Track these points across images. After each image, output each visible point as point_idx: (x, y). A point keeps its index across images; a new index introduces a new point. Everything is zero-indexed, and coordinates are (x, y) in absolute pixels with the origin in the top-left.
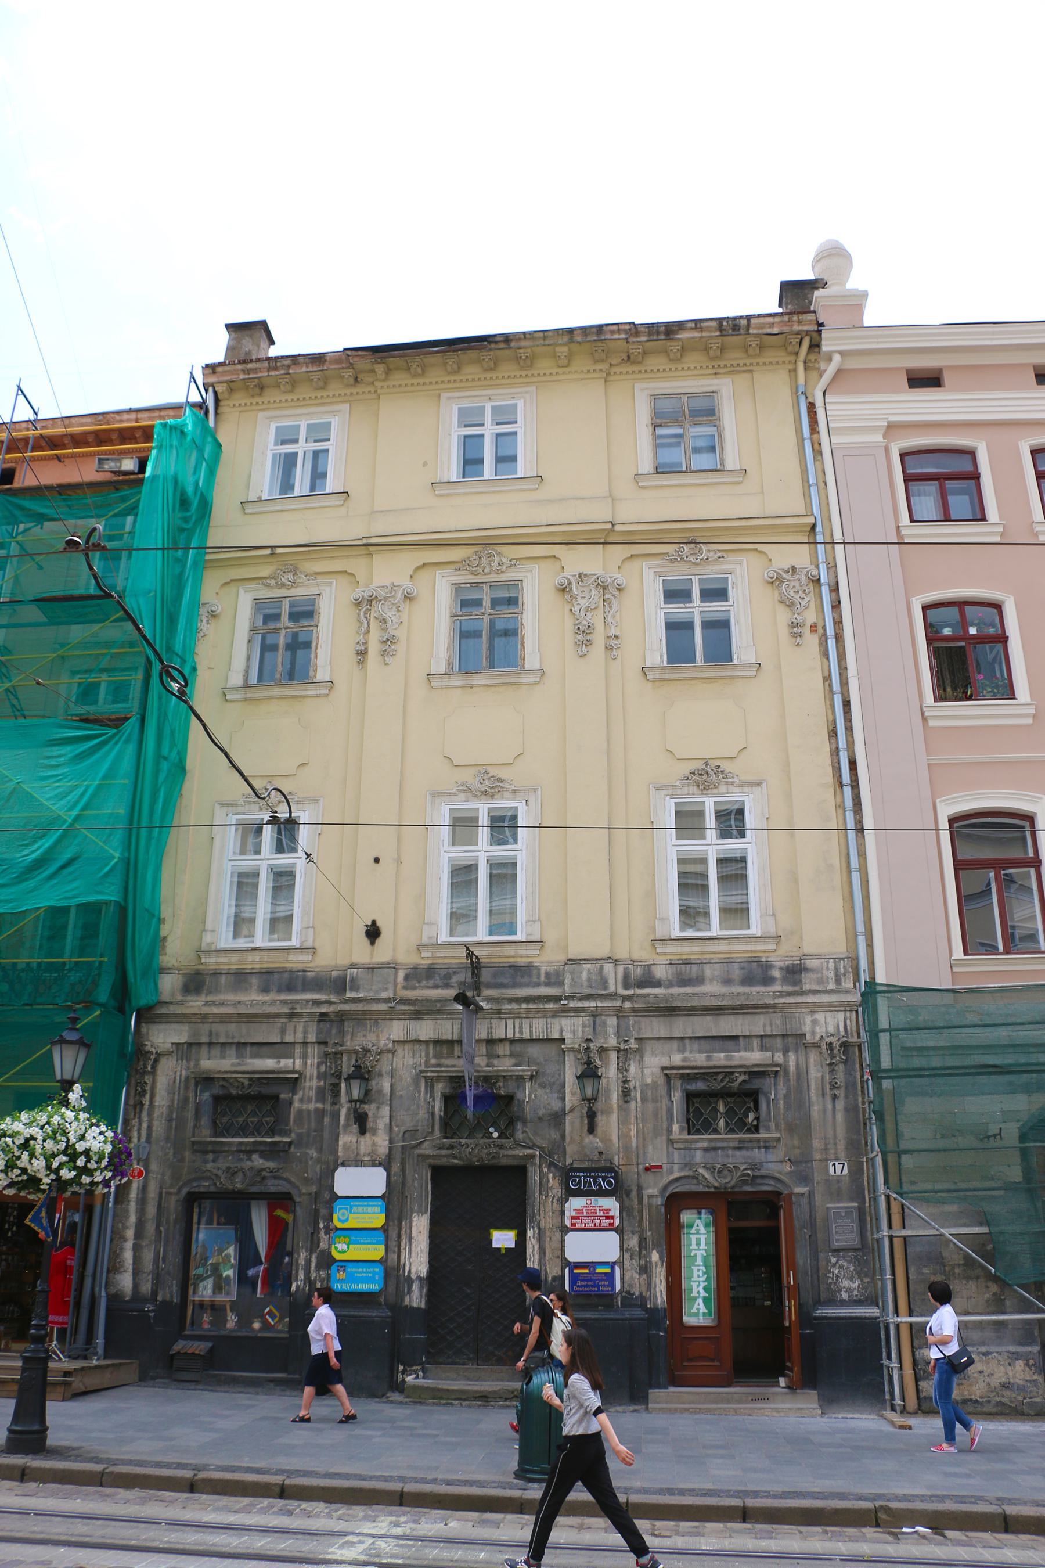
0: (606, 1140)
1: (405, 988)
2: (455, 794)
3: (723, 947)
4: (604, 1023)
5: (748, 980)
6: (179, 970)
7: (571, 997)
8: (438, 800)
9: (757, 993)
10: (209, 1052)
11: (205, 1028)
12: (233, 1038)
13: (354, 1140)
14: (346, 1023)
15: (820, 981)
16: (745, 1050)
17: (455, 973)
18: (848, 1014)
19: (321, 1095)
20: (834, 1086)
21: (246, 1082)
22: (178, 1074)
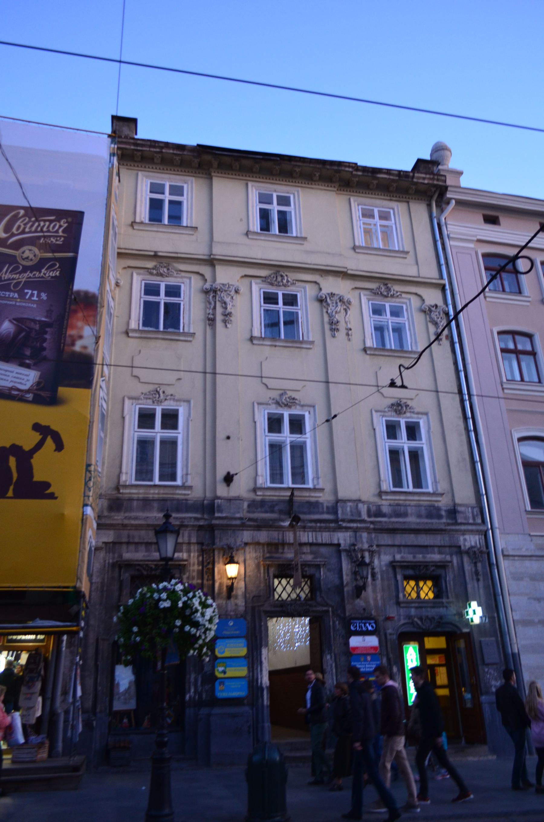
0: (367, 601)
1: (249, 512)
2: (270, 404)
3: (416, 498)
4: (361, 537)
5: (430, 516)
6: (106, 496)
7: (343, 520)
8: (261, 407)
9: (435, 523)
10: (127, 548)
11: (125, 533)
12: (144, 539)
13: (224, 602)
14: (216, 532)
15: (466, 518)
16: (431, 553)
17: (276, 505)
18: (480, 536)
19: (201, 574)
20: (477, 573)
21: (153, 567)
22: (107, 562)
